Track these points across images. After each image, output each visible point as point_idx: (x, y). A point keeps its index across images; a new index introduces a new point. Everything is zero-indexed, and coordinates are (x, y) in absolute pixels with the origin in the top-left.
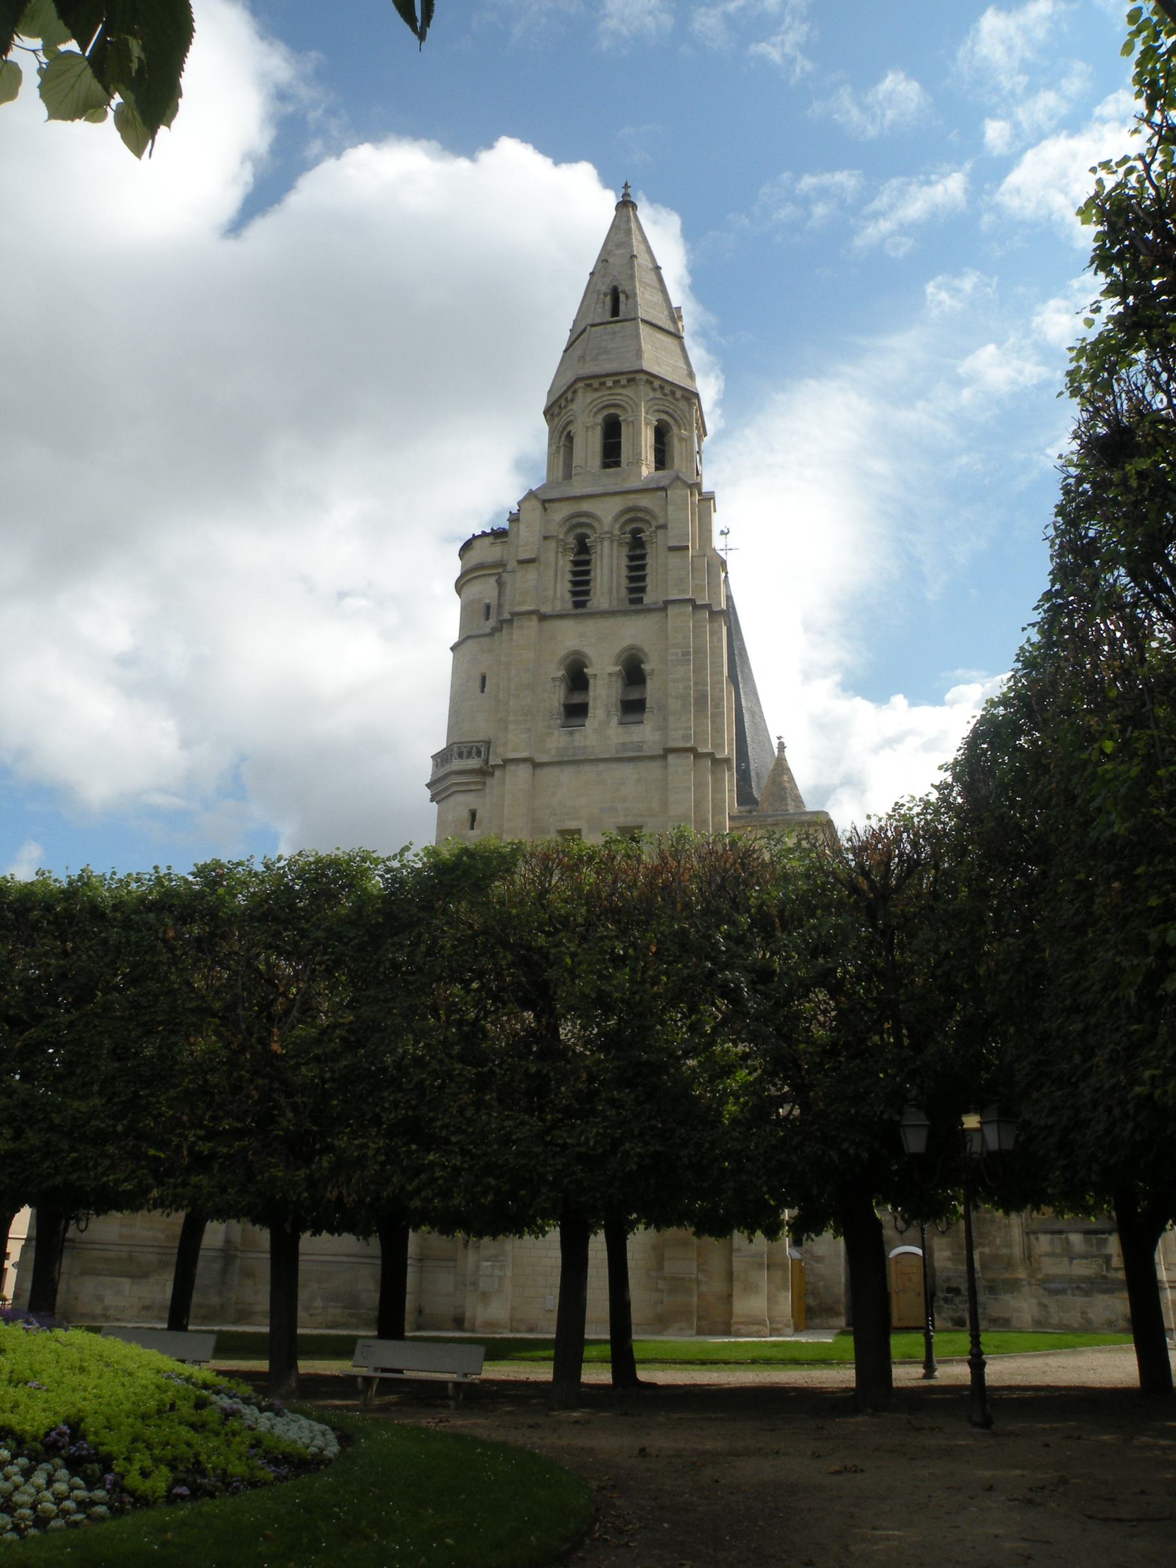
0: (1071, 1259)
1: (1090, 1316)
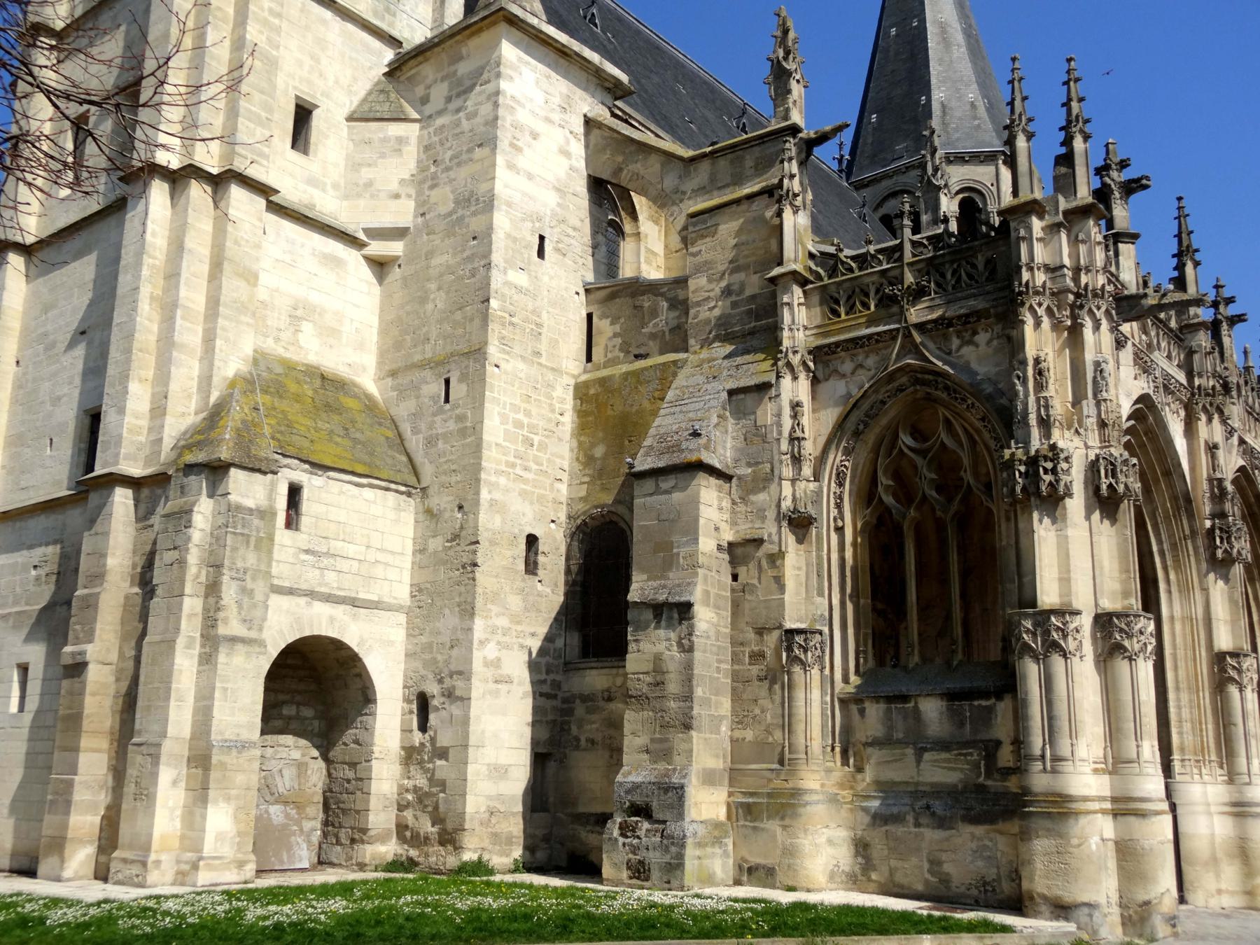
0: (920, 753)
1: (947, 868)
